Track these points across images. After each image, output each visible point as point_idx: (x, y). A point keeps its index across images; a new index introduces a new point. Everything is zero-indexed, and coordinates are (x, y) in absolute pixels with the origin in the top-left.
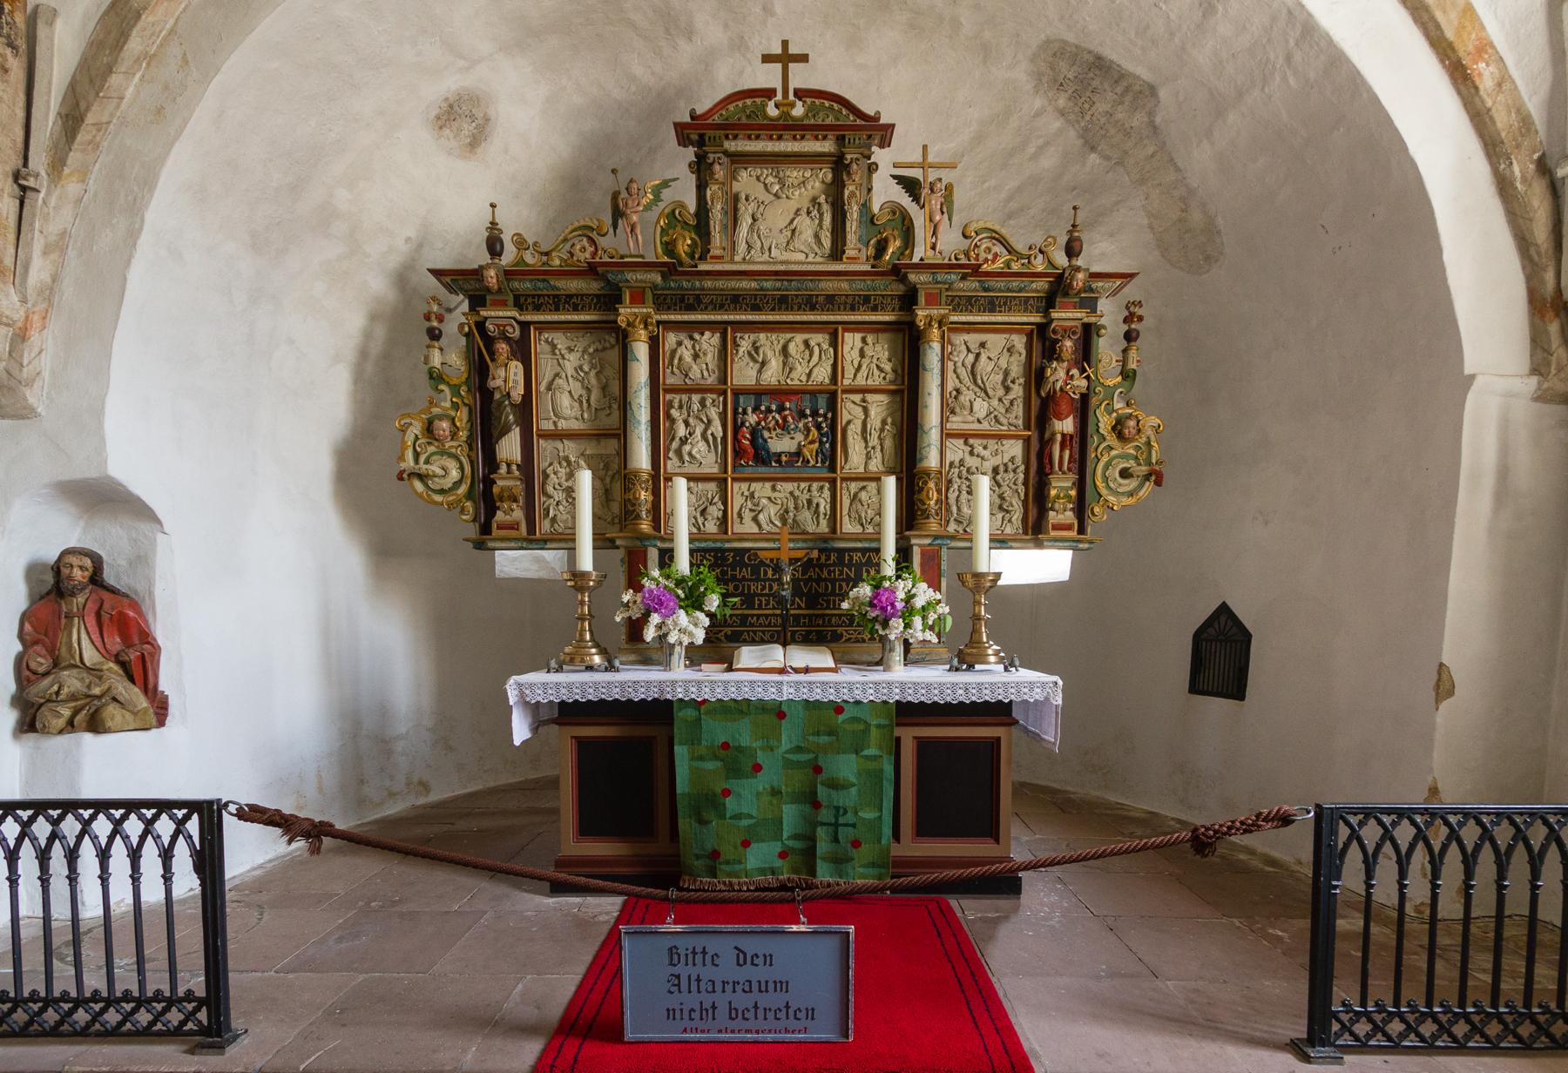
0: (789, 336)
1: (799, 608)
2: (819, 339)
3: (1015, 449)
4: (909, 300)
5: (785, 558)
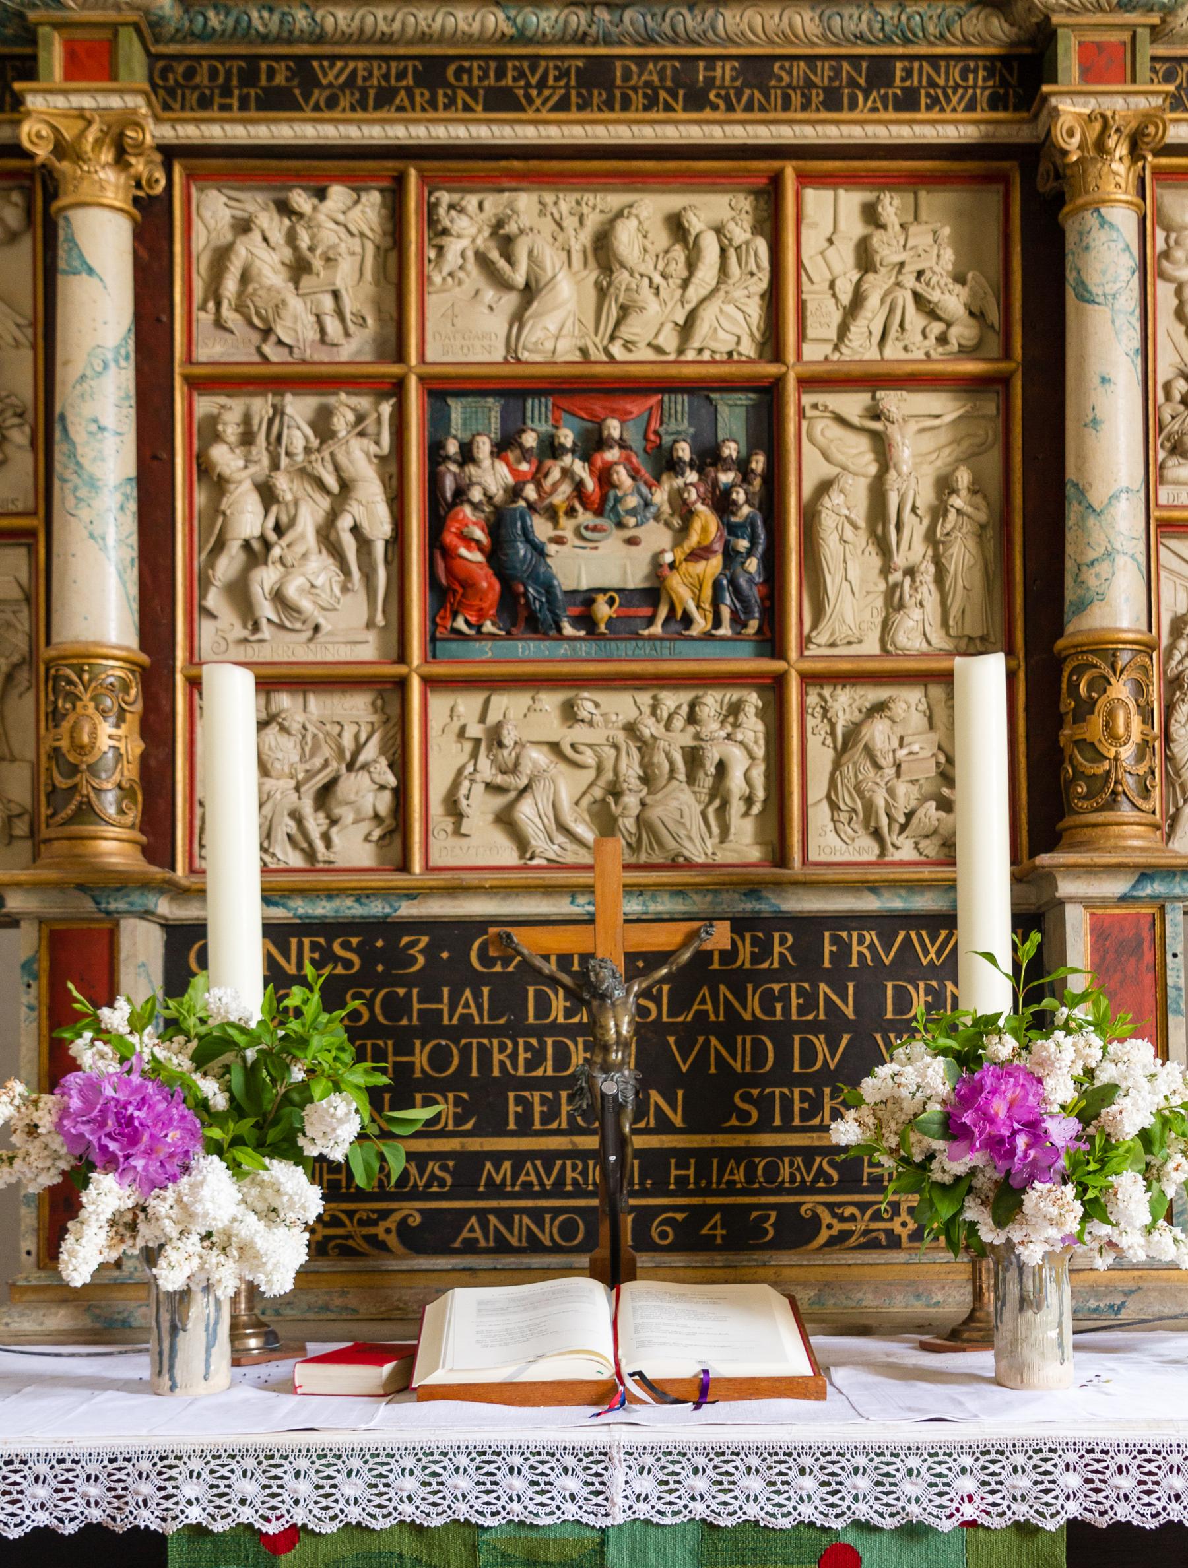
0: (614, 201)
1: (663, 1126)
2: (720, 211)
5: (609, 949)
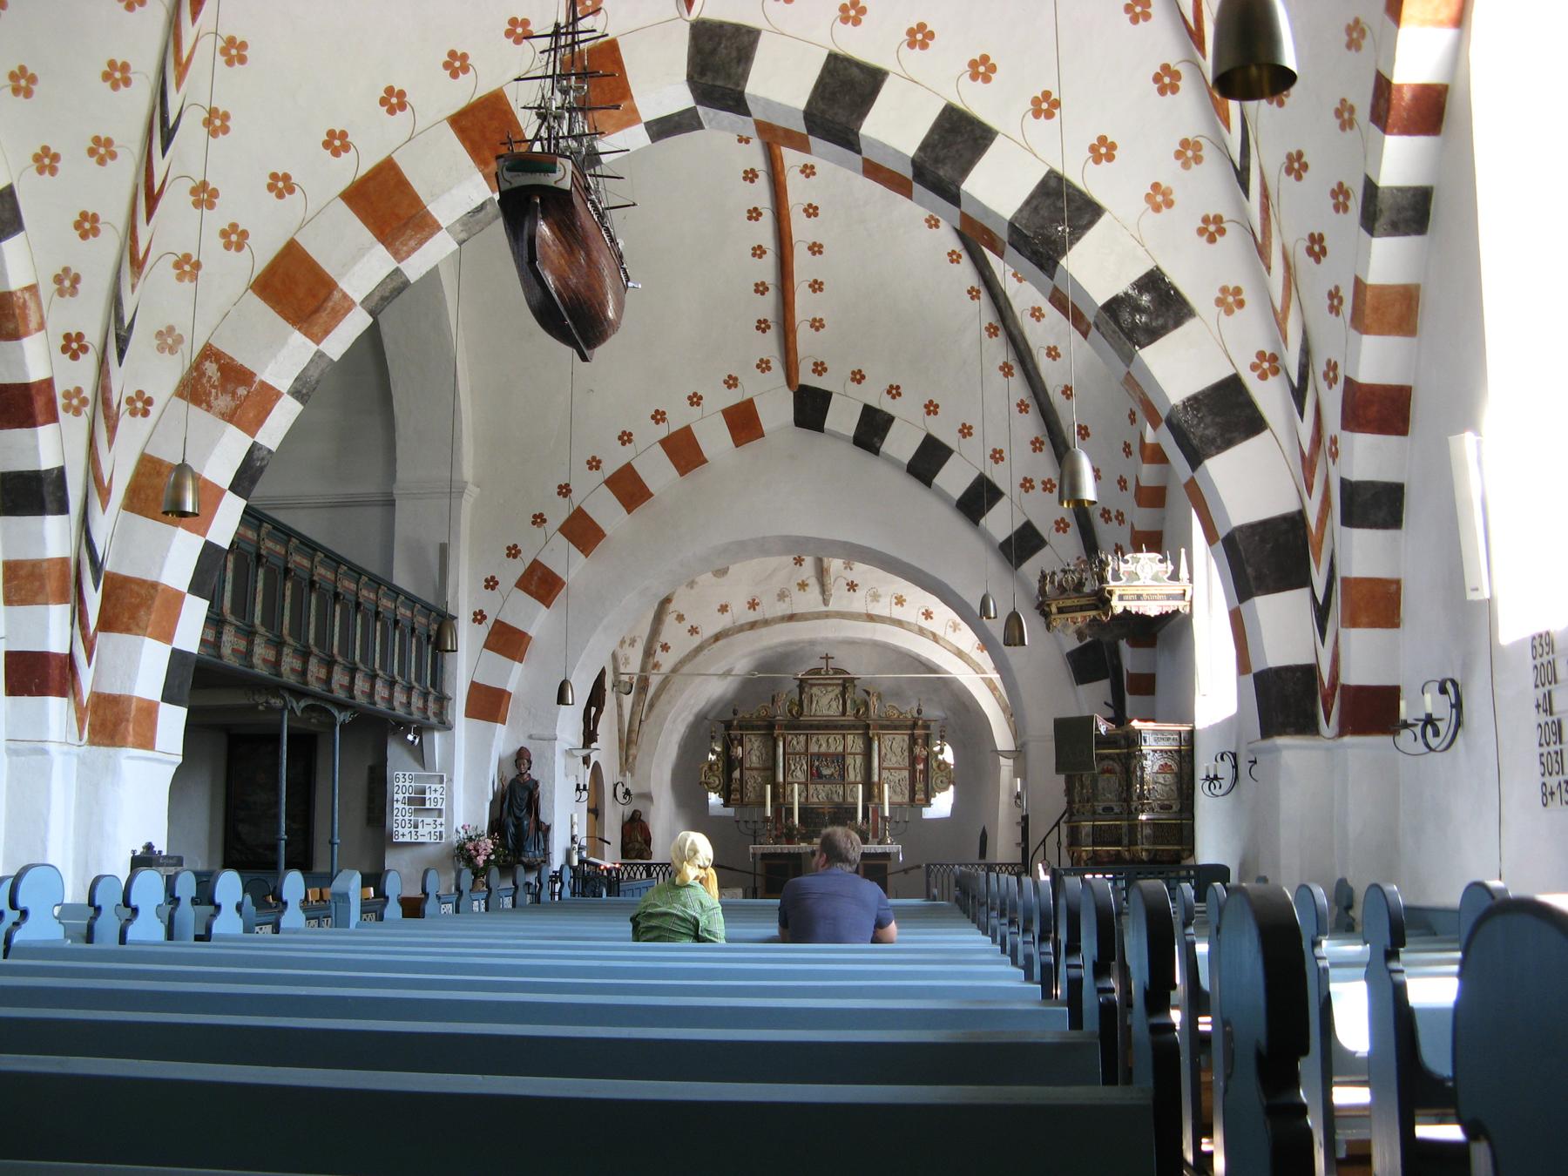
3: (906, 773)
4: (868, 727)
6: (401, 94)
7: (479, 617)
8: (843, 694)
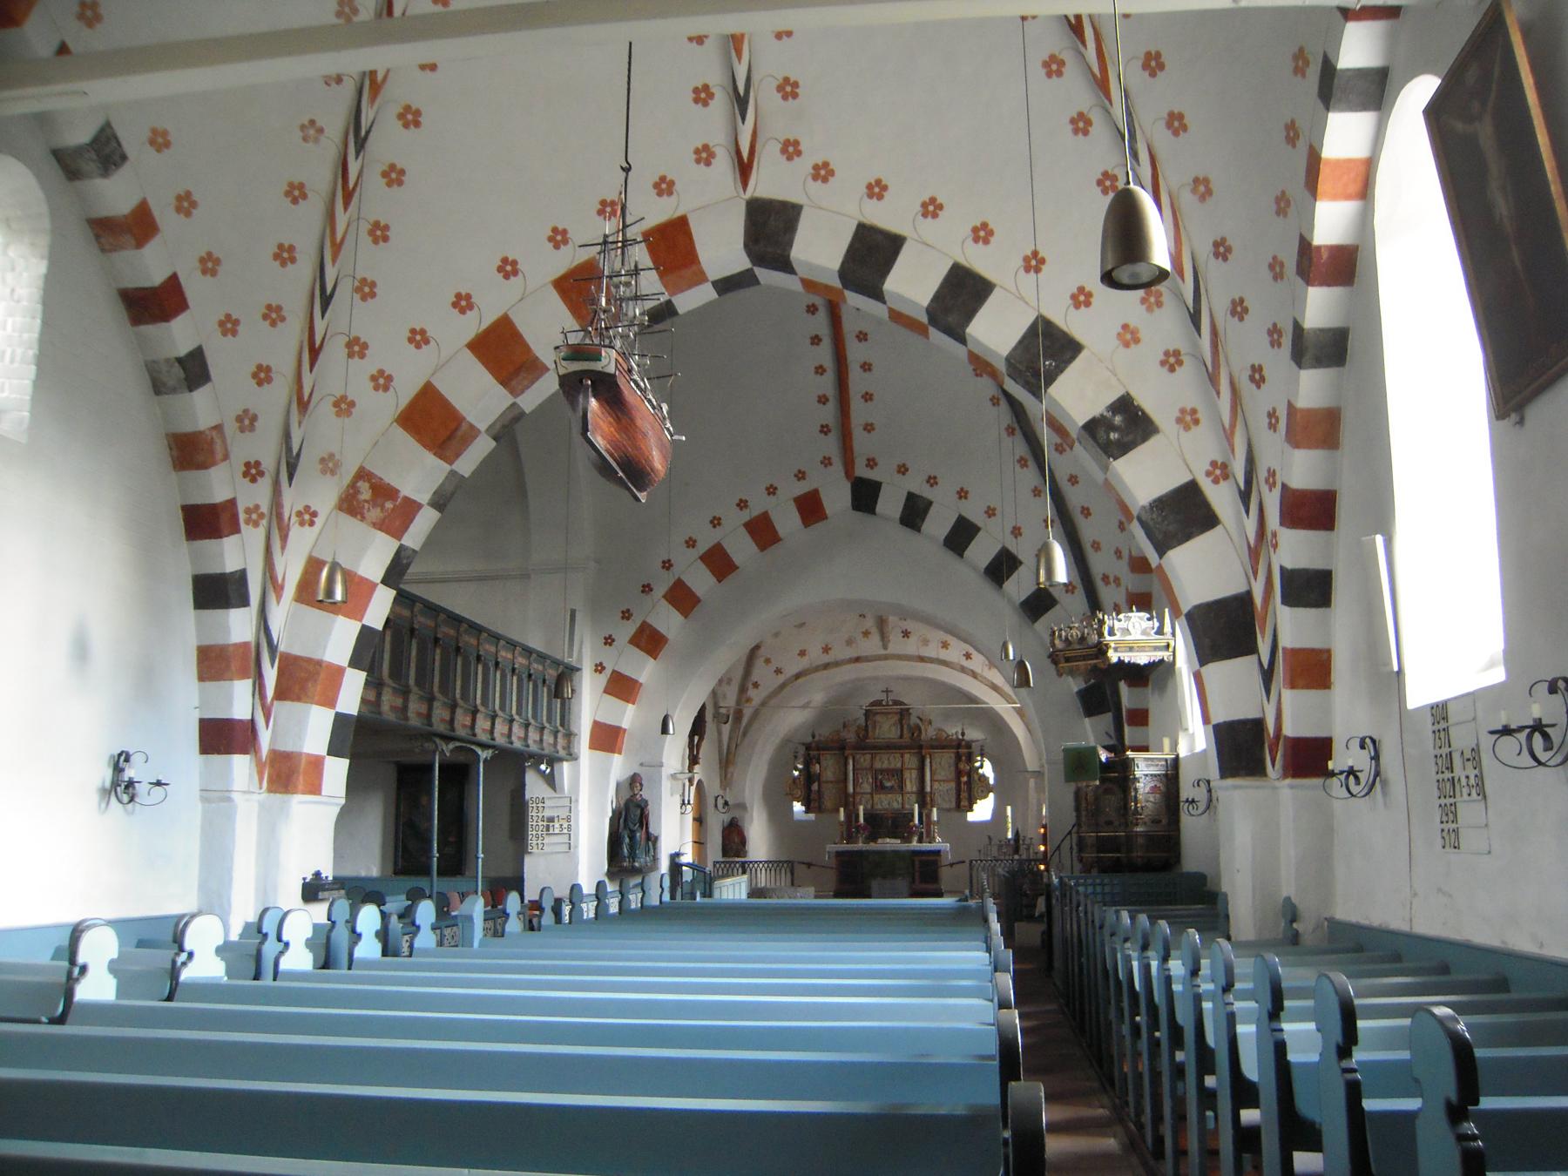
3: (953, 785)
4: (921, 747)
6: (514, 263)
7: (599, 668)
8: (901, 721)
